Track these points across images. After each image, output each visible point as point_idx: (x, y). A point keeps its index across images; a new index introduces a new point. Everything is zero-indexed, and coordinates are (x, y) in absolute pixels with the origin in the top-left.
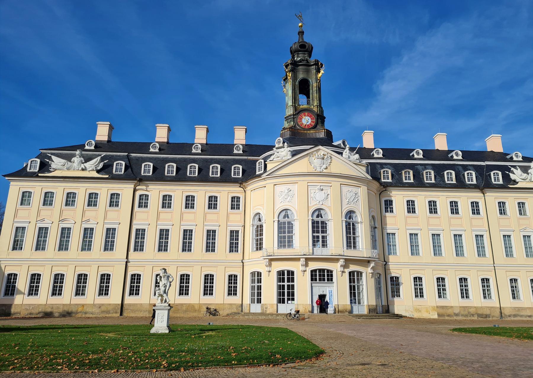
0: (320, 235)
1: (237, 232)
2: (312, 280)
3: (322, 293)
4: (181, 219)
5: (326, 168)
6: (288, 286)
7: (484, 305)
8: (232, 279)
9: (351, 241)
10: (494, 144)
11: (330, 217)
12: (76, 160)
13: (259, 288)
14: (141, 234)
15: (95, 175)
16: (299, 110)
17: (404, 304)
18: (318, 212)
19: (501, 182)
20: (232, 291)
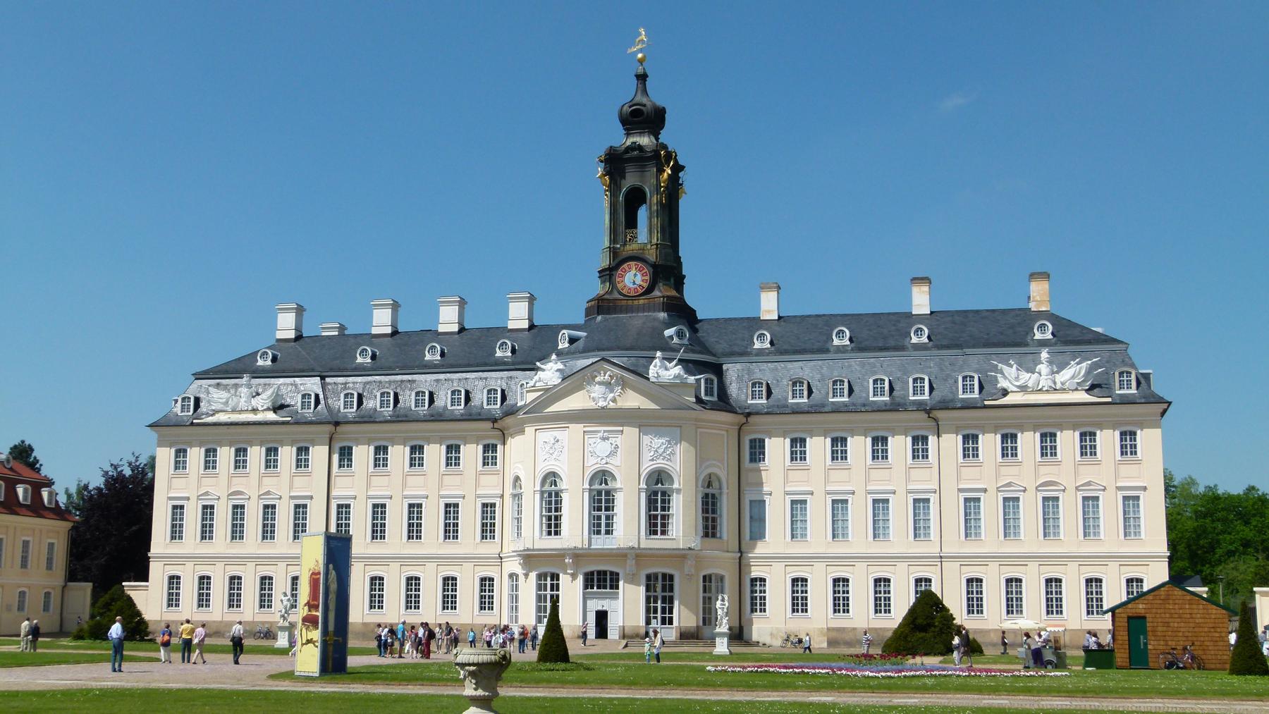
0: (603, 514)
1: (493, 505)
2: (586, 587)
3: (600, 608)
4: (404, 486)
5: (614, 400)
6: (552, 596)
7: (1008, 625)
8: (486, 582)
9: (657, 522)
10: (1039, 296)
11: (618, 485)
12: (244, 391)
15: (271, 416)
16: (624, 255)
17: (771, 625)
18: (603, 476)
19: (976, 395)
20: (486, 603)
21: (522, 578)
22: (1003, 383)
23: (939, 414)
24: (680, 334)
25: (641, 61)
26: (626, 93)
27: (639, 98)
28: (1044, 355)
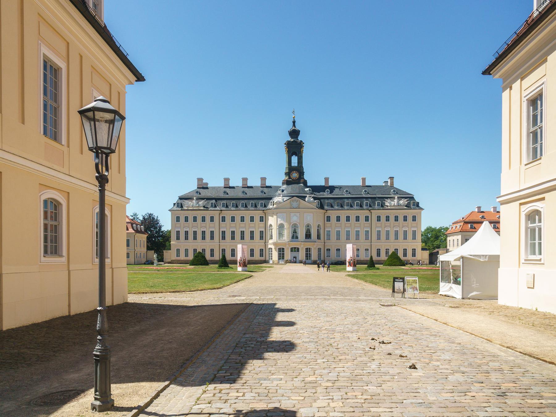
13: (272, 254)
14: (224, 233)
21: (273, 250)
22: (387, 204)
23: (372, 211)
24: (310, 190)
25: (294, 118)
26: (290, 127)
27: (294, 128)
28: (396, 198)
